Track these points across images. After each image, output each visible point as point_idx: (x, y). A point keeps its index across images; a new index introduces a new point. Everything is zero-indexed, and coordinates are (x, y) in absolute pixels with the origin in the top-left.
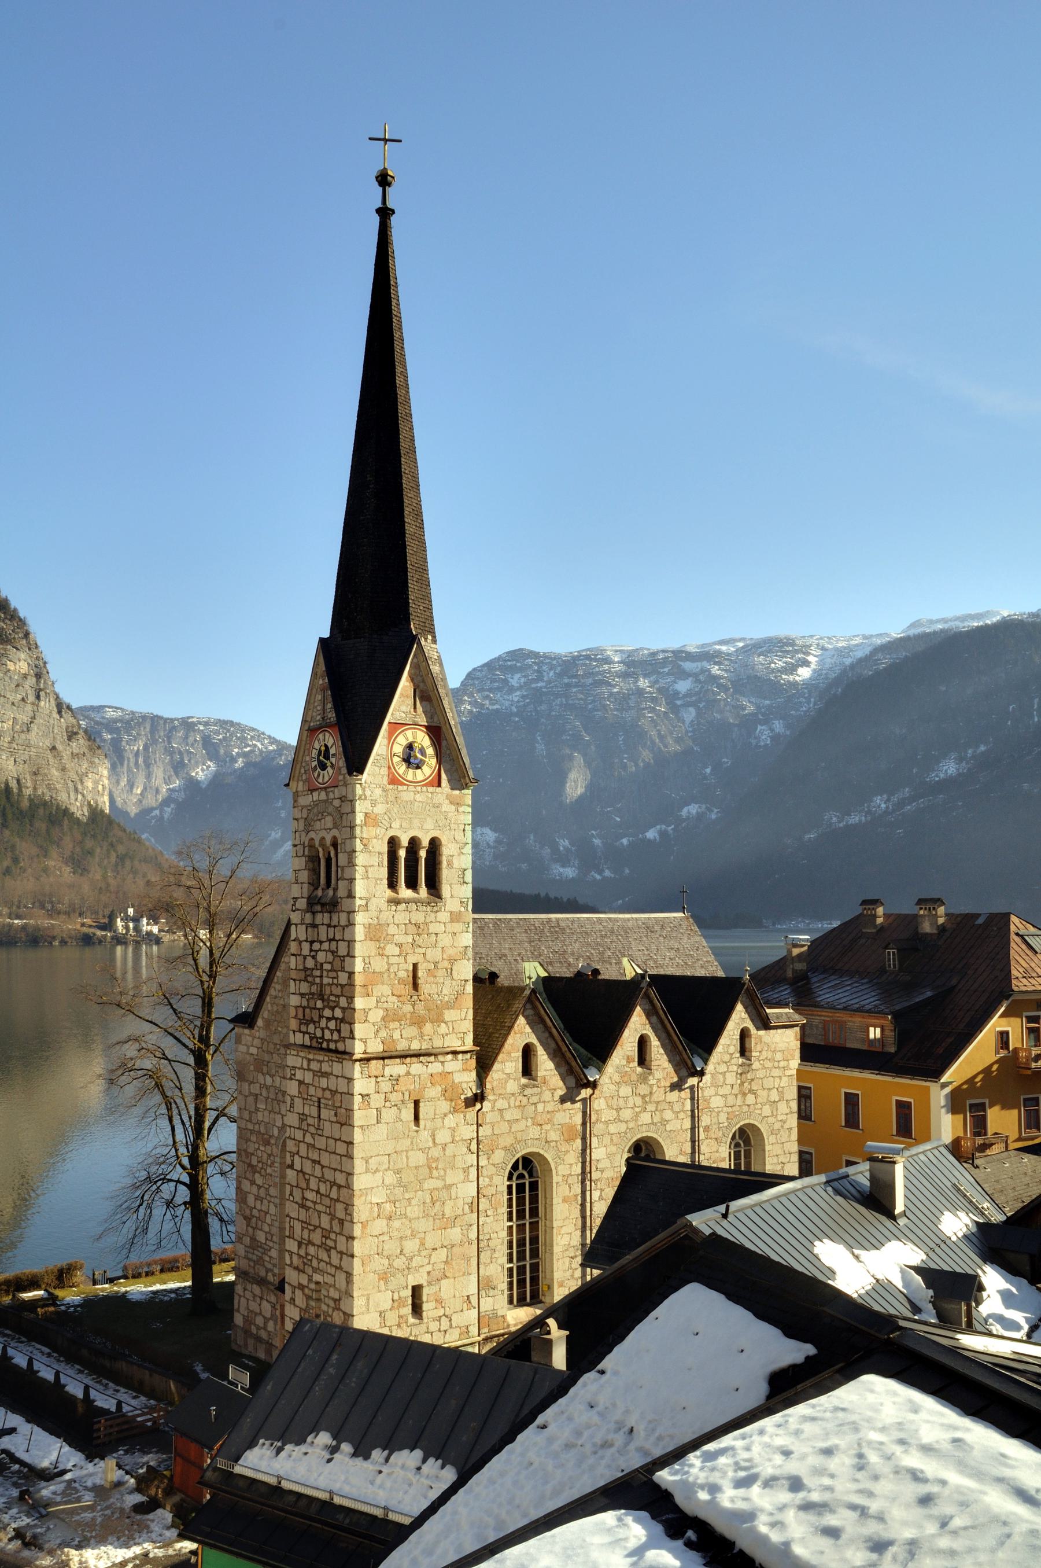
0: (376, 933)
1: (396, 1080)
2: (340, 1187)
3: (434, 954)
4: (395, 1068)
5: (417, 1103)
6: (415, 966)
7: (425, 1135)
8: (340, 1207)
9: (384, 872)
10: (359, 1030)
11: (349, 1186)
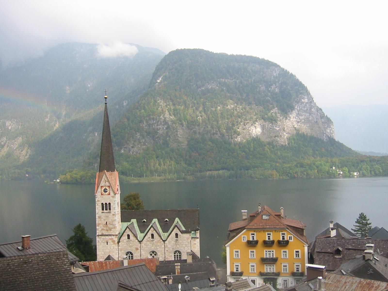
0: (100, 217)
4: (103, 237)
5: (107, 242)
6: (107, 222)
9: (101, 208)
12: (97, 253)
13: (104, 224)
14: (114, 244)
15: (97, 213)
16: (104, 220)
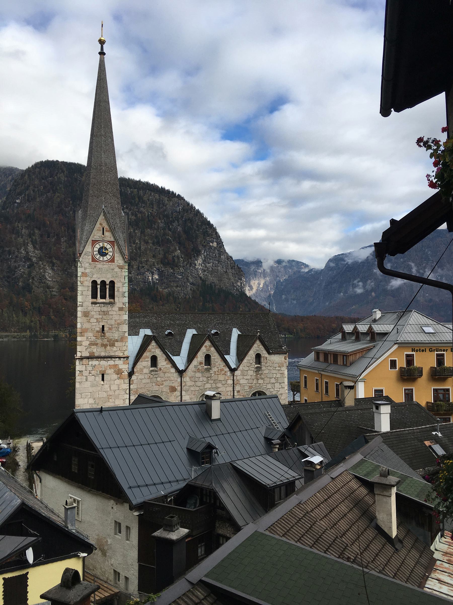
0: (86, 314)
3: (113, 322)
4: (95, 362)
5: (103, 375)
7: (106, 386)
9: (90, 293)
10: (79, 349)
15: (81, 304)
16: (98, 321)
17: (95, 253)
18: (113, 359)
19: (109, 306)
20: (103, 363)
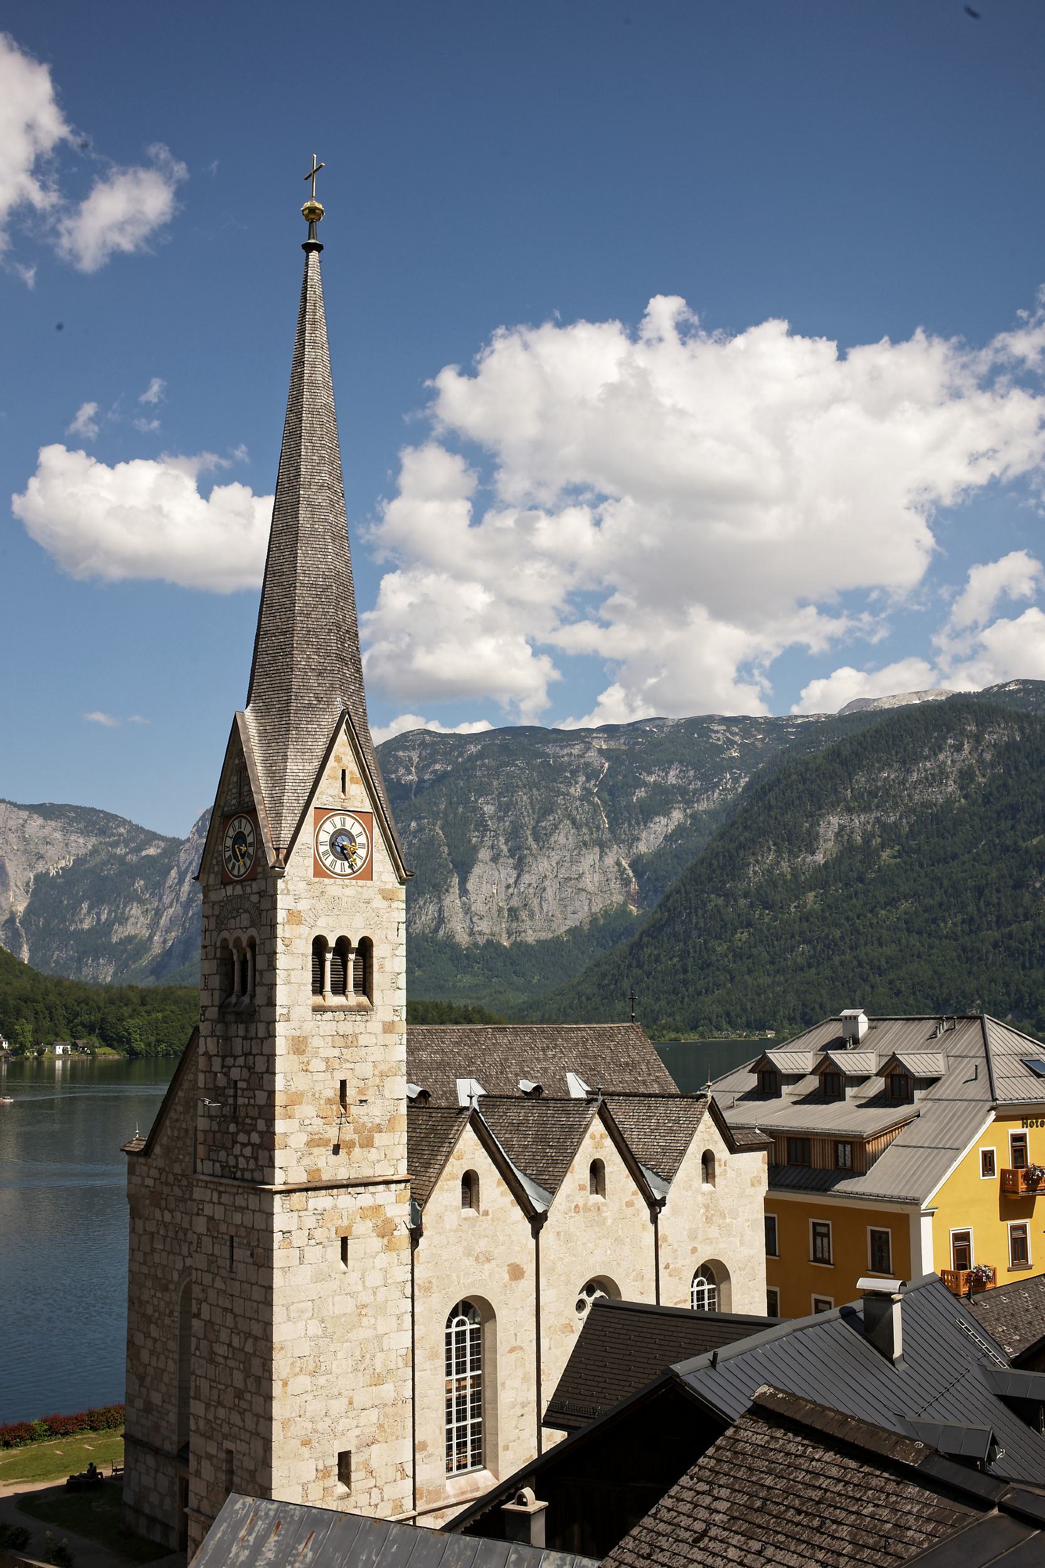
0: (299, 1046)
1: (321, 1214)
2: (256, 1338)
3: (366, 1070)
4: (321, 1201)
5: (344, 1241)
6: (343, 1083)
7: (353, 1277)
8: (256, 1362)
9: (308, 977)
10: (280, 1157)
11: (268, 1337)
12: (277, 1338)
13: (329, 1101)
14: (388, 1248)
15: (285, 1011)
17: (322, 849)
18: (371, 1189)
19: (359, 1018)
20: (345, 1200)
